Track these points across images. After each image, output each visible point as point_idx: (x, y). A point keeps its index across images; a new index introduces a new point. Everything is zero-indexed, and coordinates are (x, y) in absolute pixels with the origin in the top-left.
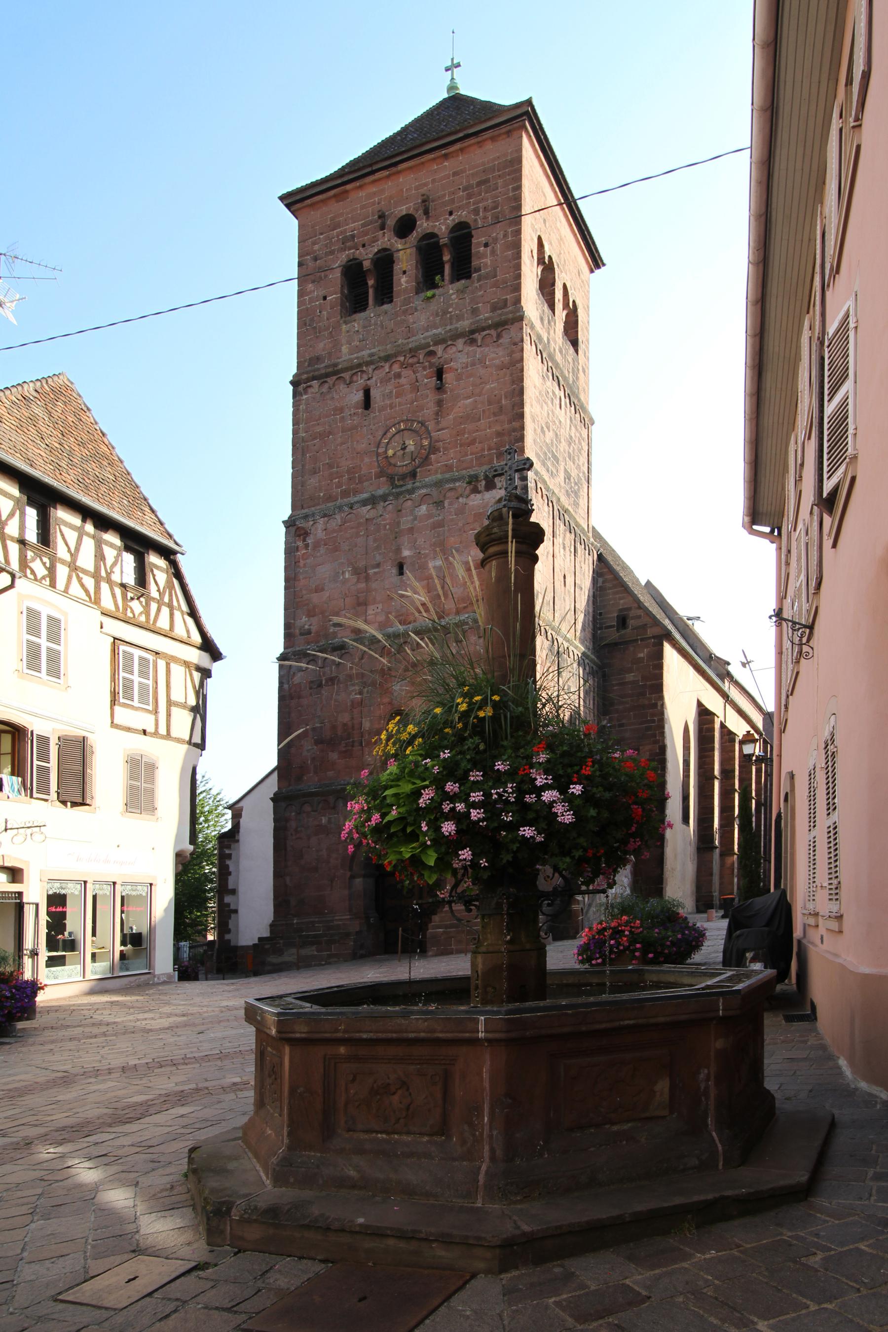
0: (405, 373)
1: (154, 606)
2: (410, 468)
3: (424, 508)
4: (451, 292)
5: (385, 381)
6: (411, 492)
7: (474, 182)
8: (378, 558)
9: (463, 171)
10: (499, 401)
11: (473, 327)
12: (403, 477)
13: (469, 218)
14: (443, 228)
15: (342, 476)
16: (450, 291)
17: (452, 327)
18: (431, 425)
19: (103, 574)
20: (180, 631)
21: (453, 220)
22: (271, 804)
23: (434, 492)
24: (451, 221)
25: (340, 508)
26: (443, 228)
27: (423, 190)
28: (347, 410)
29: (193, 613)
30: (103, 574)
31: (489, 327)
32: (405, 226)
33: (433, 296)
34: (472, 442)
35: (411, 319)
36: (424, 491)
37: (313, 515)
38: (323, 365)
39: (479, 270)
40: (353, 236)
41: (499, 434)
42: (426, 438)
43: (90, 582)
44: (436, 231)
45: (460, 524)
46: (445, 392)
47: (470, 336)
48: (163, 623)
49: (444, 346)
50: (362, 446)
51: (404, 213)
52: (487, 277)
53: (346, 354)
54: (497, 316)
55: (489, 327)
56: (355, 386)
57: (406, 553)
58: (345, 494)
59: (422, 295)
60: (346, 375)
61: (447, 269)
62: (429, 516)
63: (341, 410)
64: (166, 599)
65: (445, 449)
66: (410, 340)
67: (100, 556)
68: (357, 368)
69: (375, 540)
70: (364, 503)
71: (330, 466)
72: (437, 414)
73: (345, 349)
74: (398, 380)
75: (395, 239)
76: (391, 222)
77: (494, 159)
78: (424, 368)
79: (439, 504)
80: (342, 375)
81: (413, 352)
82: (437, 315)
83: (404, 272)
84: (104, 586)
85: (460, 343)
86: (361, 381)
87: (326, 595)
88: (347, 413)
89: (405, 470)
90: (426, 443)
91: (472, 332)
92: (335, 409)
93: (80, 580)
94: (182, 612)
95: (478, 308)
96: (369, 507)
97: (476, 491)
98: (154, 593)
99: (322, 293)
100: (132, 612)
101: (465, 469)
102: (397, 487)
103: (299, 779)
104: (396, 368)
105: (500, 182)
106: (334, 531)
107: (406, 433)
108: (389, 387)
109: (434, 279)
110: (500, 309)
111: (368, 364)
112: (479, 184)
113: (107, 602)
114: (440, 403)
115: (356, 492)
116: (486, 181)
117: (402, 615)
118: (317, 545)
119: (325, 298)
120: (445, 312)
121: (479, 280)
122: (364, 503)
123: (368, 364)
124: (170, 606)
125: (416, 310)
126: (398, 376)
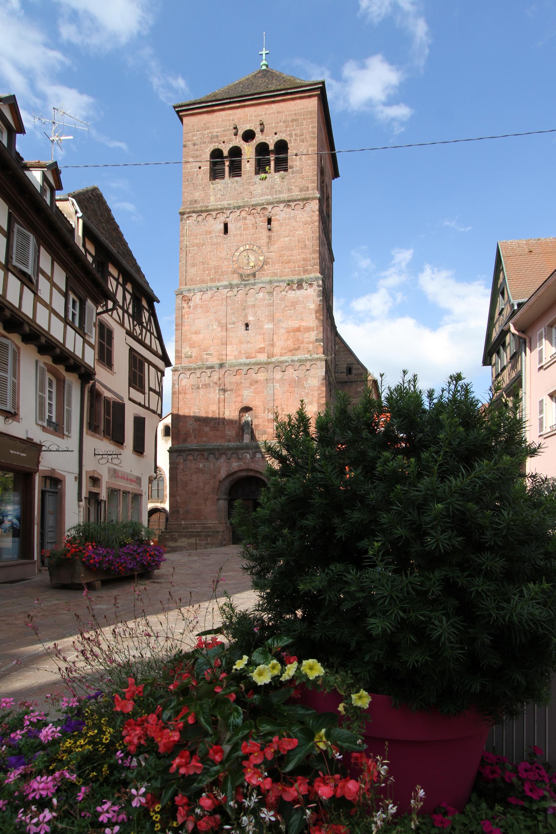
0: (249, 217)
1: (144, 331)
2: (252, 271)
3: (261, 295)
4: (276, 177)
5: (237, 220)
6: (254, 284)
7: (289, 119)
8: (234, 319)
9: (283, 112)
10: (304, 242)
11: (290, 198)
12: (249, 275)
13: (287, 139)
14: (272, 141)
15: (211, 270)
16: (274, 177)
17: (277, 196)
18: (265, 249)
19: (126, 308)
20: (154, 347)
21: (277, 138)
22: (168, 453)
23: (268, 286)
24: (277, 138)
25: (211, 288)
26: (272, 141)
27: (260, 118)
28: (214, 233)
29: (159, 338)
30: (126, 308)
31: (299, 200)
32: (249, 136)
33: (266, 178)
34: (289, 262)
35: (252, 188)
36: (261, 285)
37: (194, 290)
38: (199, 206)
39: (293, 168)
40: (217, 136)
41: (304, 260)
42: (262, 256)
43: (120, 311)
44: (267, 142)
45: (283, 306)
46: (273, 232)
47: (288, 203)
48: (147, 342)
49: (272, 206)
50: (223, 255)
51: (248, 129)
52: (297, 172)
53: (213, 203)
54: (303, 195)
55: (299, 200)
56: (218, 220)
57: (250, 318)
58: (213, 280)
59: (259, 176)
60: (214, 213)
61: (272, 163)
62: (264, 299)
63: (210, 232)
64: (149, 328)
65: (273, 263)
66: (252, 199)
67: (124, 298)
68: (221, 210)
69: (232, 309)
70: (225, 287)
71: (203, 263)
72: (268, 243)
73: (212, 198)
74: (244, 221)
75: (242, 142)
76: (241, 132)
77: (301, 109)
78: (261, 217)
79: (270, 293)
80: (211, 213)
81: (254, 206)
82: (268, 188)
83: (248, 161)
84: (126, 315)
85: (282, 205)
86: (222, 218)
87: (201, 336)
88: (214, 235)
89: (248, 272)
90: (261, 258)
91: (289, 201)
92: (206, 232)
93: (117, 310)
94: (155, 336)
95: (291, 189)
96: (228, 290)
97: (292, 289)
98: (145, 324)
99: (199, 164)
100: (136, 333)
101: (285, 276)
102: (244, 280)
103: (185, 440)
104: (244, 214)
105: (305, 122)
106: (206, 301)
107: (249, 251)
108: (240, 224)
109: (265, 168)
110: (305, 191)
111: (227, 209)
112: (293, 121)
113: (127, 325)
114: (269, 237)
115: (219, 280)
116: (296, 120)
117: (248, 353)
118: (196, 307)
119: (200, 168)
120: (272, 188)
121: (292, 173)
122: (225, 287)
123: (227, 209)
124: (149, 331)
125: (255, 184)
126: (245, 218)
